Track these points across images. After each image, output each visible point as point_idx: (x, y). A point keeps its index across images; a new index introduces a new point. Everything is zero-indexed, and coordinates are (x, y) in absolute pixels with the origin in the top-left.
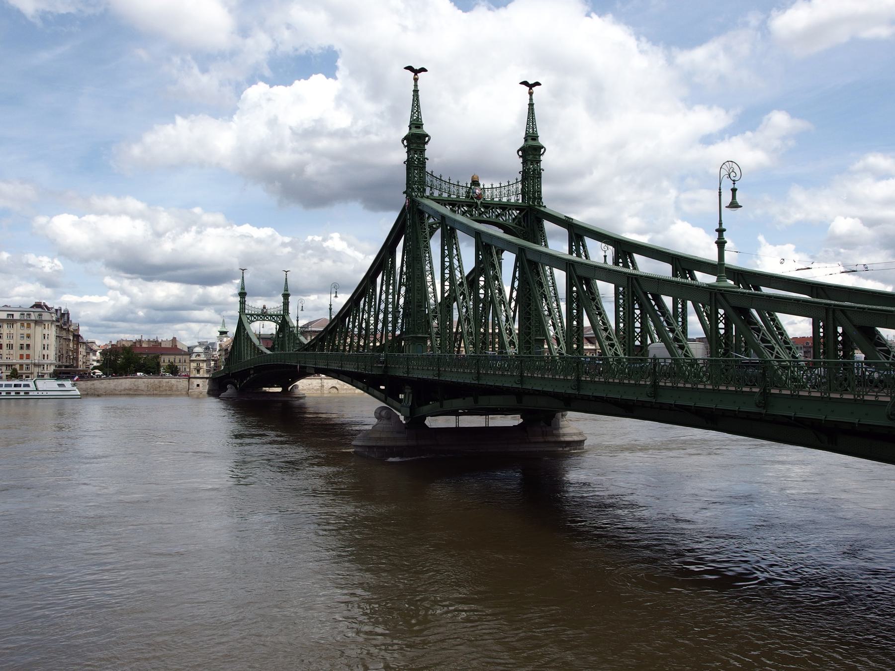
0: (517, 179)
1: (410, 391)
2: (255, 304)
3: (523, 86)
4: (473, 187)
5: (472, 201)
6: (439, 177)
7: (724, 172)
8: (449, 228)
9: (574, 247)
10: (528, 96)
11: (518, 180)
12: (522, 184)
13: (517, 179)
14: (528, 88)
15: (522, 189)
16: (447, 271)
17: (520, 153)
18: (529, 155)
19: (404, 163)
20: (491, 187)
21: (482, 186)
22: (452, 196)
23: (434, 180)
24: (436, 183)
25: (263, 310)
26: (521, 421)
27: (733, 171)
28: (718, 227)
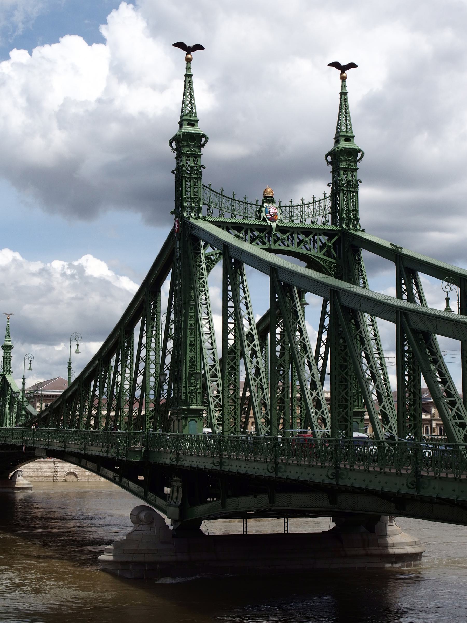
0: (325, 194)
1: (179, 484)
4: (265, 205)
5: (265, 223)
6: (220, 192)
8: (233, 261)
9: (404, 286)
11: (327, 195)
12: (332, 200)
13: (325, 194)
14: (340, 71)
15: (332, 208)
16: (231, 320)
17: (329, 158)
18: (342, 161)
19: (173, 172)
26: (333, 525)
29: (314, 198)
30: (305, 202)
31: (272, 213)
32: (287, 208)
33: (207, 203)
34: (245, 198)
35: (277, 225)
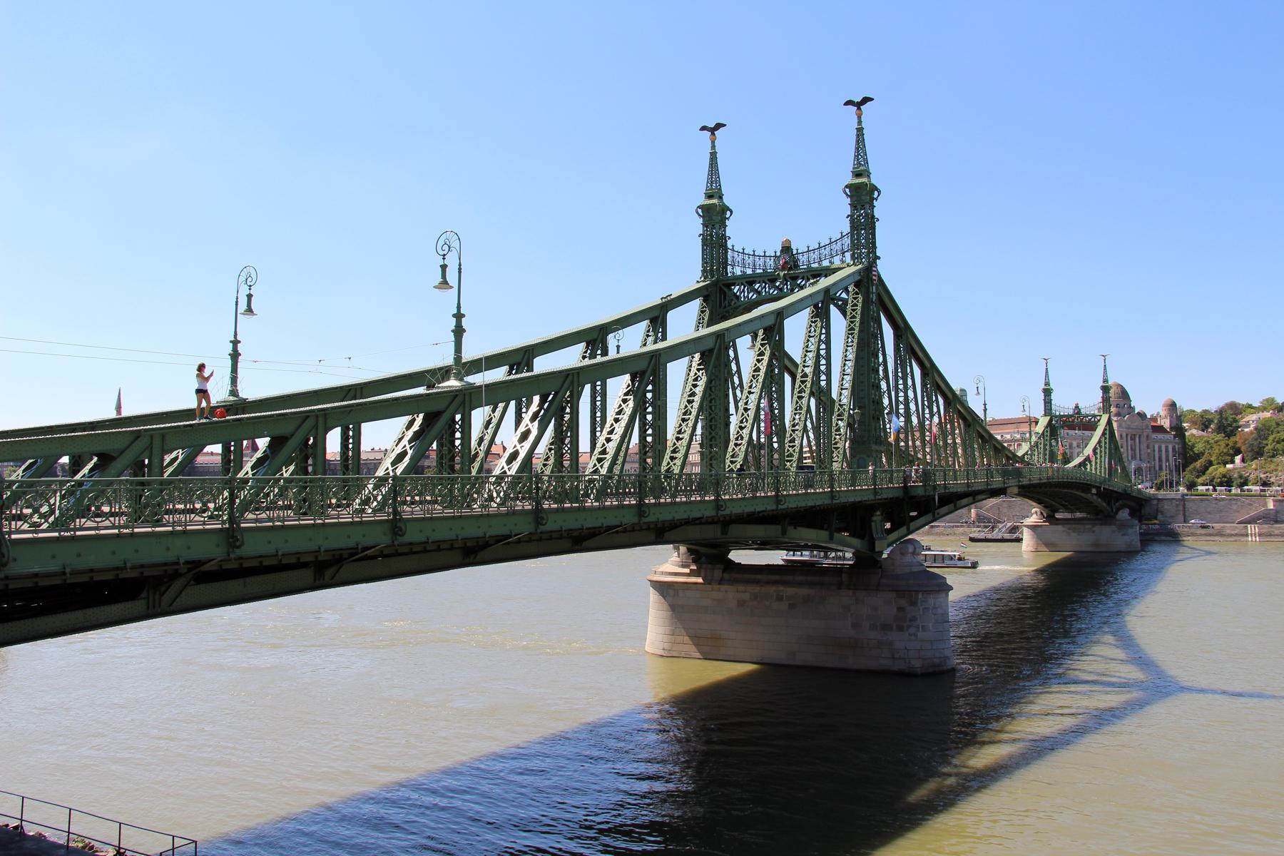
0: (842, 233)
2: (1063, 405)
6: (741, 251)
7: (242, 279)
14: (856, 108)
21: (795, 252)
22: (758, 271)
24: (739, 258)
25: (1074, 410)
28: (233, 339)
29: (830, 239)
34: (765, 252)
35: (784, 274)
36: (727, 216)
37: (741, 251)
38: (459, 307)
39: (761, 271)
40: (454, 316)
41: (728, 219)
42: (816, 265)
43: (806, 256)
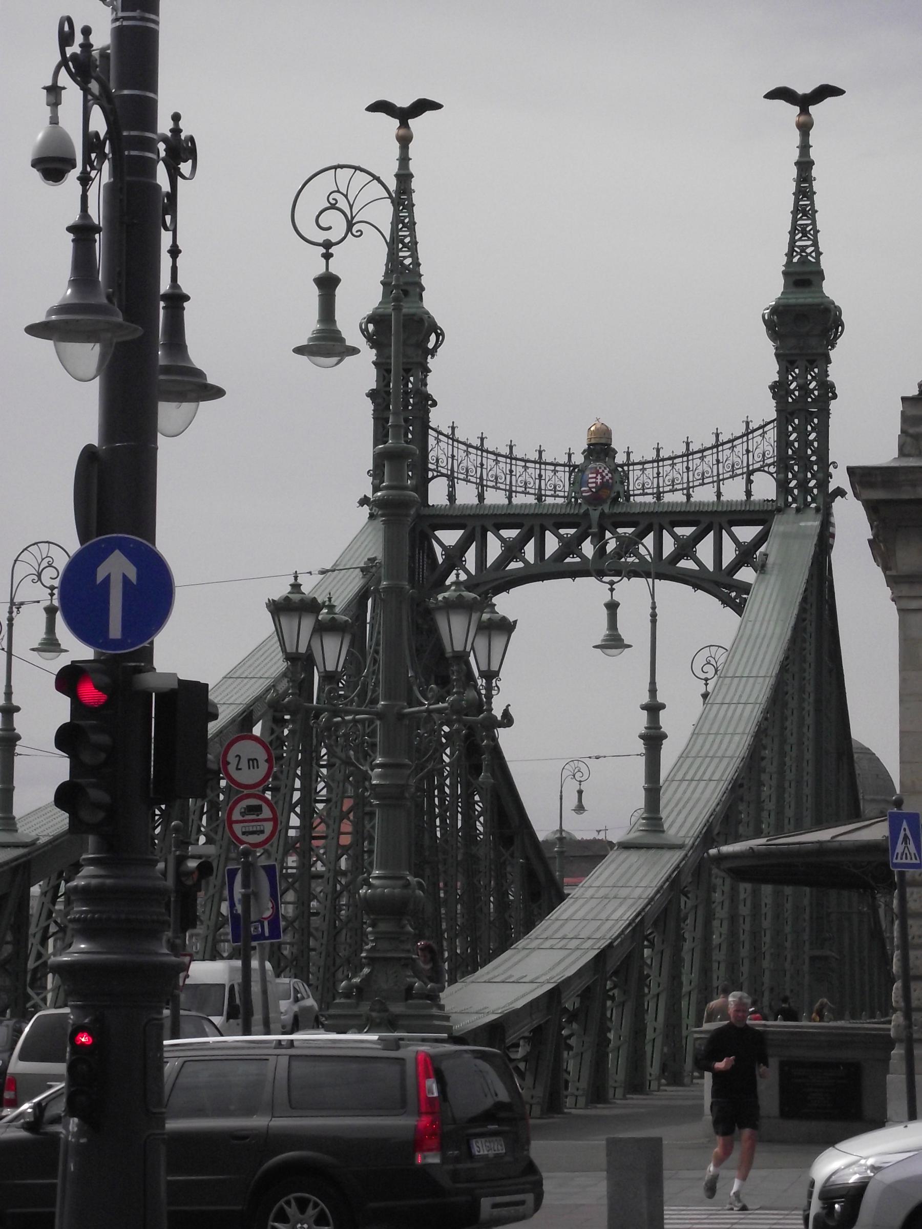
0: (747, 423)
3: (780, 104)
6: (477, 443)
7: (22, 570)
10: (796, 138)
20: (652, 455)
21: (620, 459)
22: (518, 500)
23: (460, 454)
27: (50, 566)
30: (694, 447)
31: (594, 485)
32: (646, 466)
33: (444, 471)
34: (540, 452)
35: (602, 514)
36: (431, 345)
37: (477, 443)
38: (653, 691)
39: (531, 500)
40: (644, 708)
41: (433, 352)
42: (678, 497)
43: (650, 472)
